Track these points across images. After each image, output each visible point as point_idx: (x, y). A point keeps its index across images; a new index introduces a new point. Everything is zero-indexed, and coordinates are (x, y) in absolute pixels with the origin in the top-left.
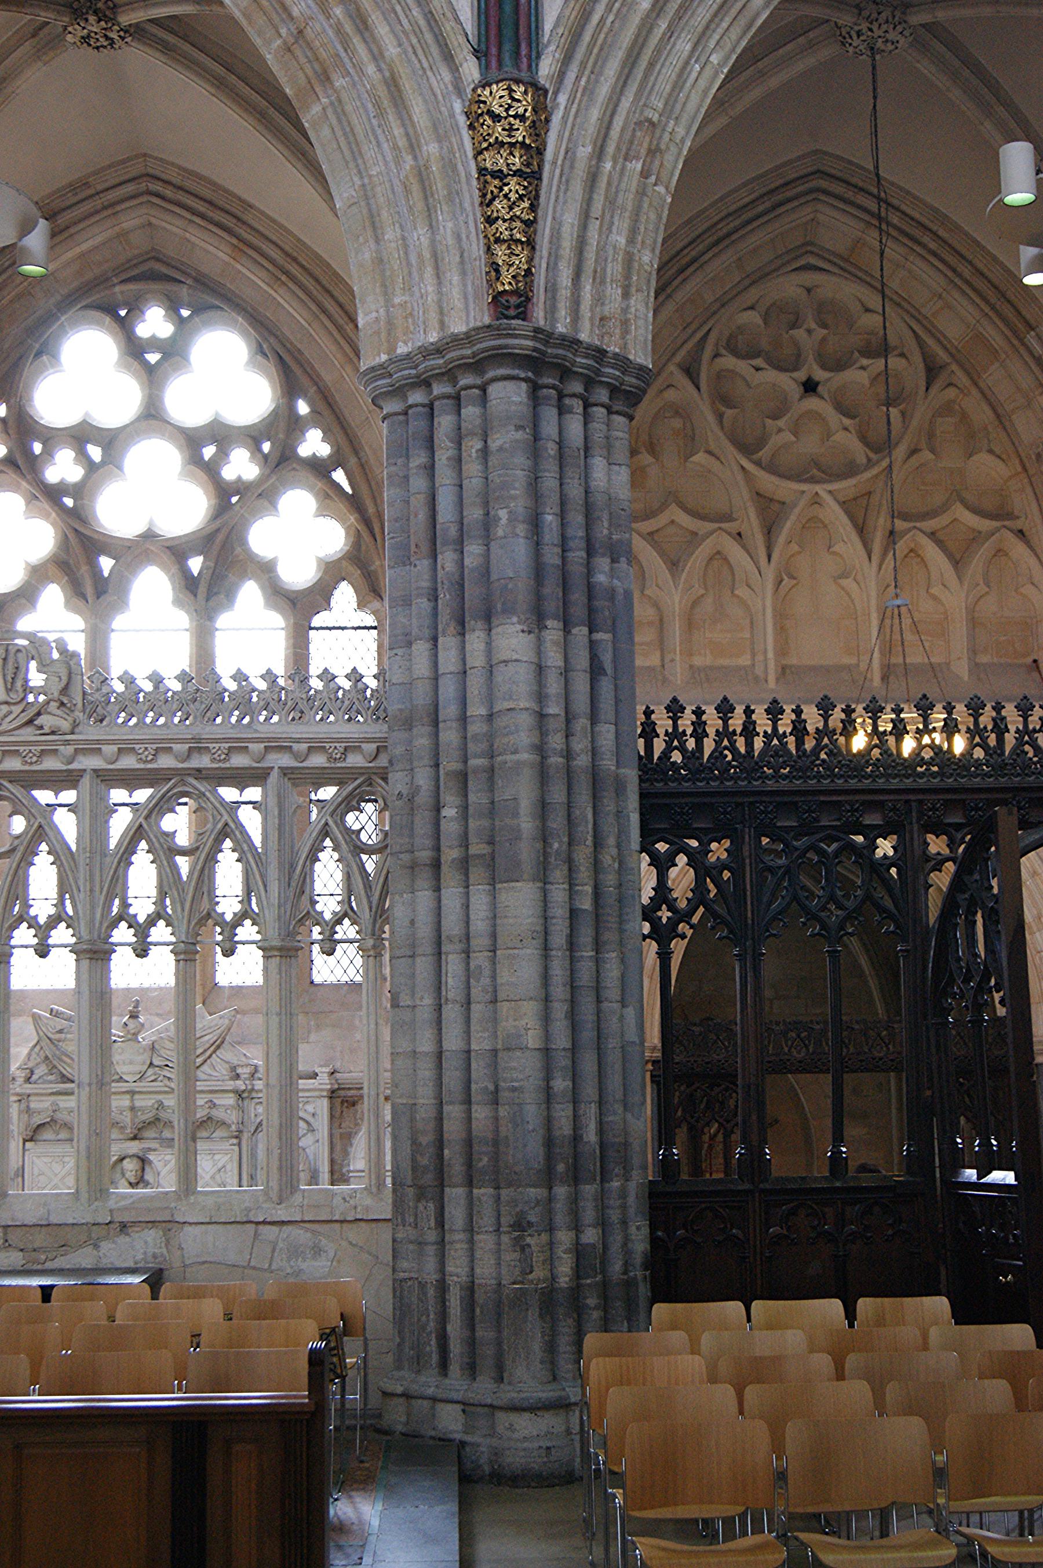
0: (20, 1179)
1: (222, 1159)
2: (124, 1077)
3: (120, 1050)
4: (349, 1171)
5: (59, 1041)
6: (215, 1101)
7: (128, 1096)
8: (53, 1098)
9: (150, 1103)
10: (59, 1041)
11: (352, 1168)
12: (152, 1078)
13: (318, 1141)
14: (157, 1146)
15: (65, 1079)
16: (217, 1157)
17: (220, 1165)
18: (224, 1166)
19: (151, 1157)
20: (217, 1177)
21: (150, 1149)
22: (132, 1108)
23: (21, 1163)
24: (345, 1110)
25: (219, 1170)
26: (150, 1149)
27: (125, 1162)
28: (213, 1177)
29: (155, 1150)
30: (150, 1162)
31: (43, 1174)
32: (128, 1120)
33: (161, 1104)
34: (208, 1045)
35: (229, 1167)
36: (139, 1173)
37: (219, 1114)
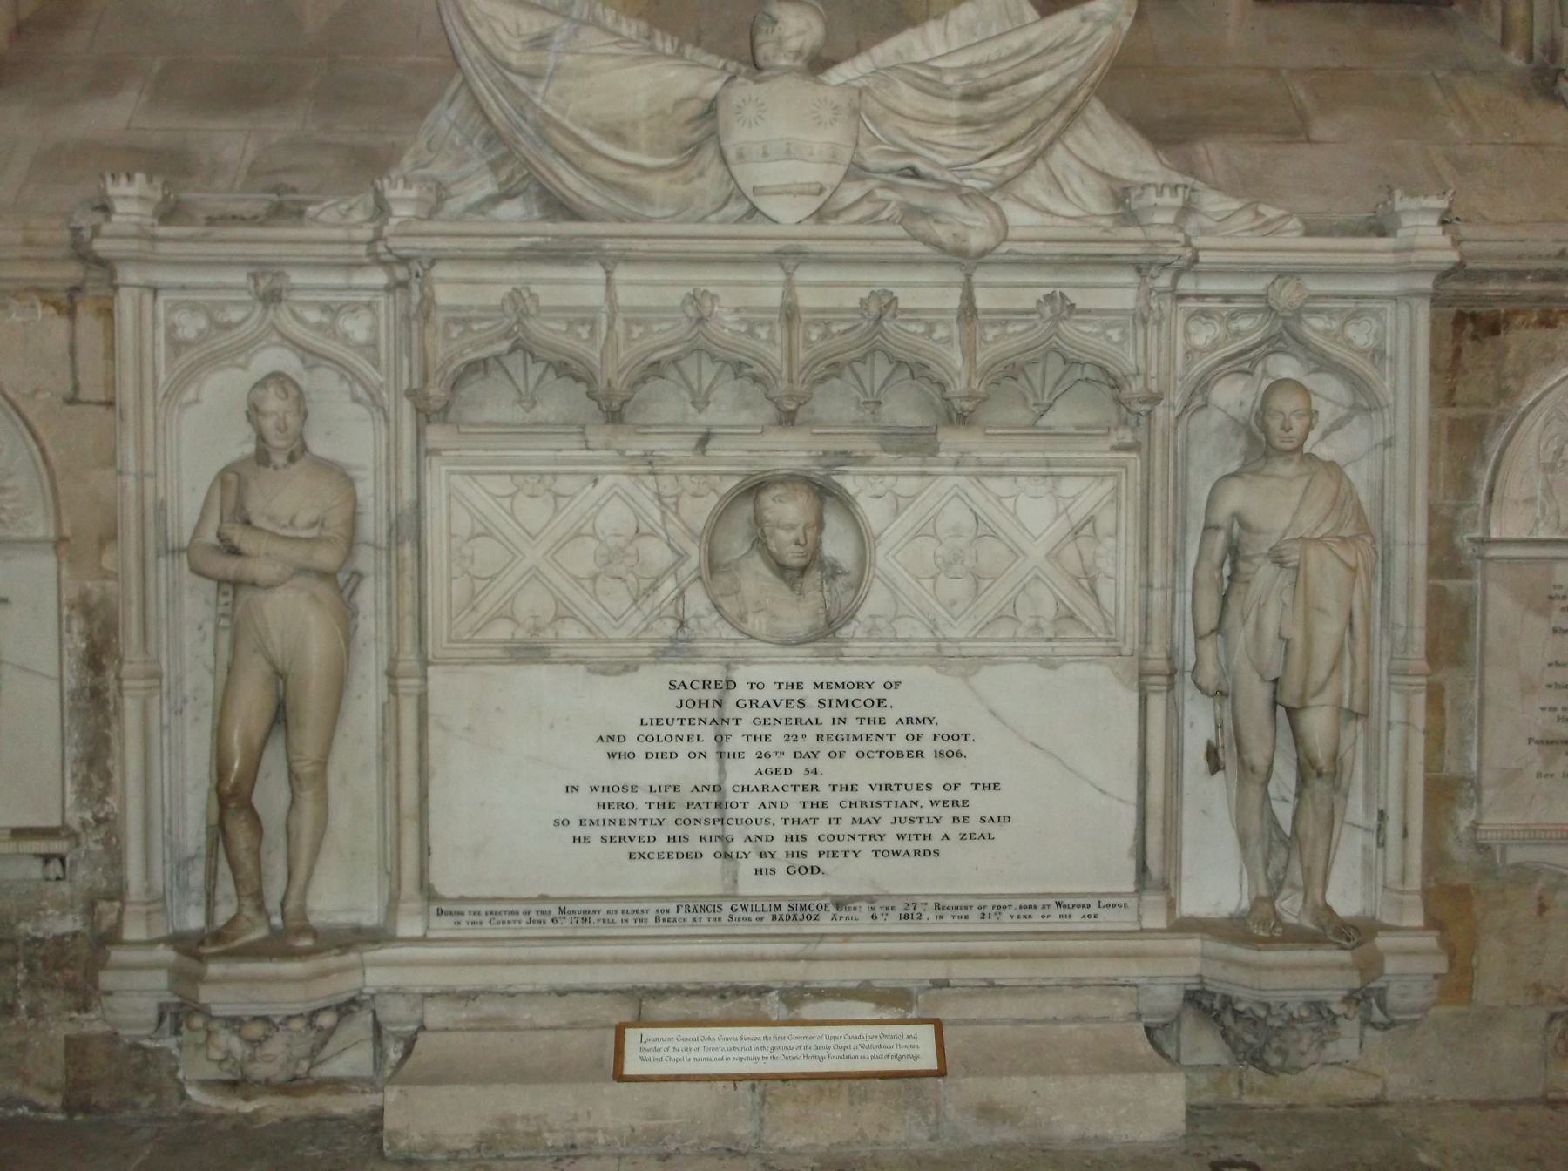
0: (408, 550)
1: (1085, 495)
2: (767, 205)
3: (750, 112)
4: (1485, 542)
5: (533, 76)
6: (1074, 296)
7: (778, 275)
8: (515, 273)
9: (852, 298)
10: (533, 76)
11: (1494, 534)
12: (865, 210)
13: (1388, 443)
14: (871, 446)
15: (558, 206)
16: (1069, 487)
17: (1078, 514)
18: (1091, 519)
19: (851, 482)
20: (1070, 553)
21: (847, 457)
22: (789, 314)
23: (408, 494)
24: (1468, 344)
25: (1076, 532)
26: (847, 457)
27: (767, 499)
28: (1054, 556)
29: (864, 460)
30: (846, 503)
31: (487, 534)
32: (776, 355)
33: (886, 305)
34: (1046, 107)
35: (1106, 522)
36: (810, 534)
37: (1080, 335)
